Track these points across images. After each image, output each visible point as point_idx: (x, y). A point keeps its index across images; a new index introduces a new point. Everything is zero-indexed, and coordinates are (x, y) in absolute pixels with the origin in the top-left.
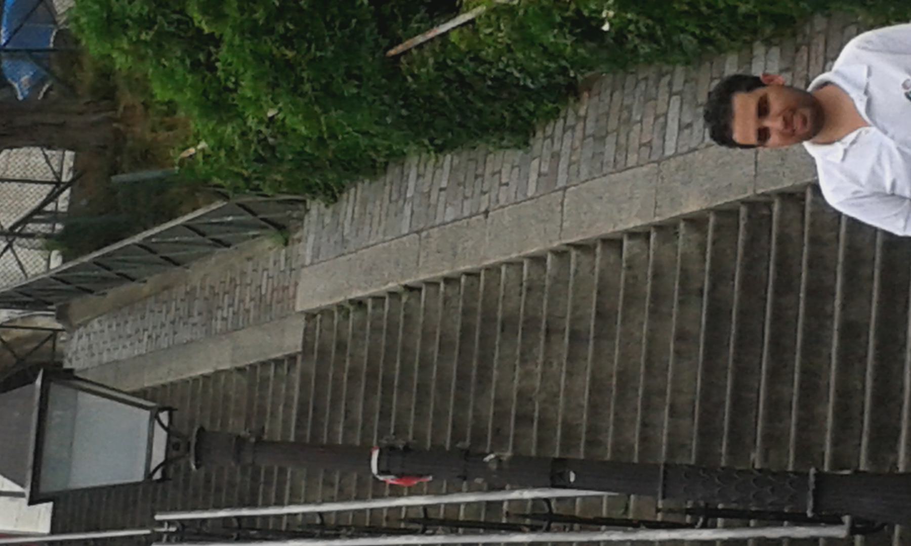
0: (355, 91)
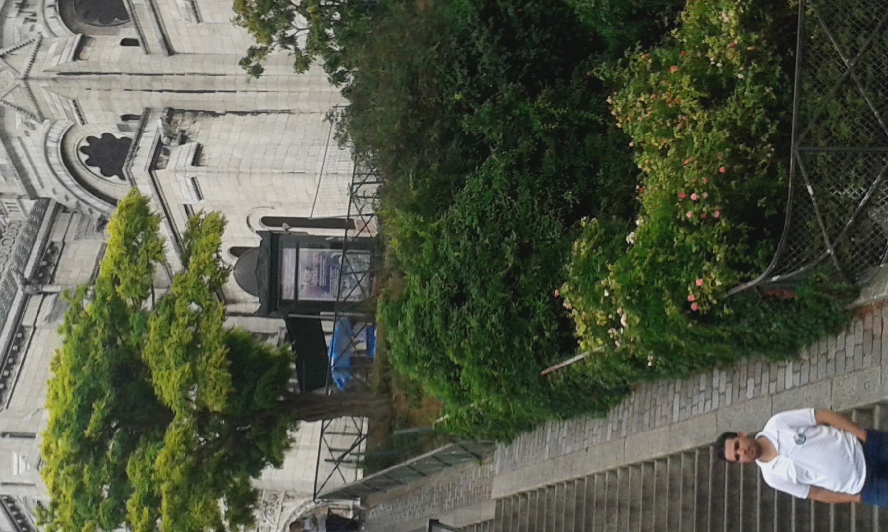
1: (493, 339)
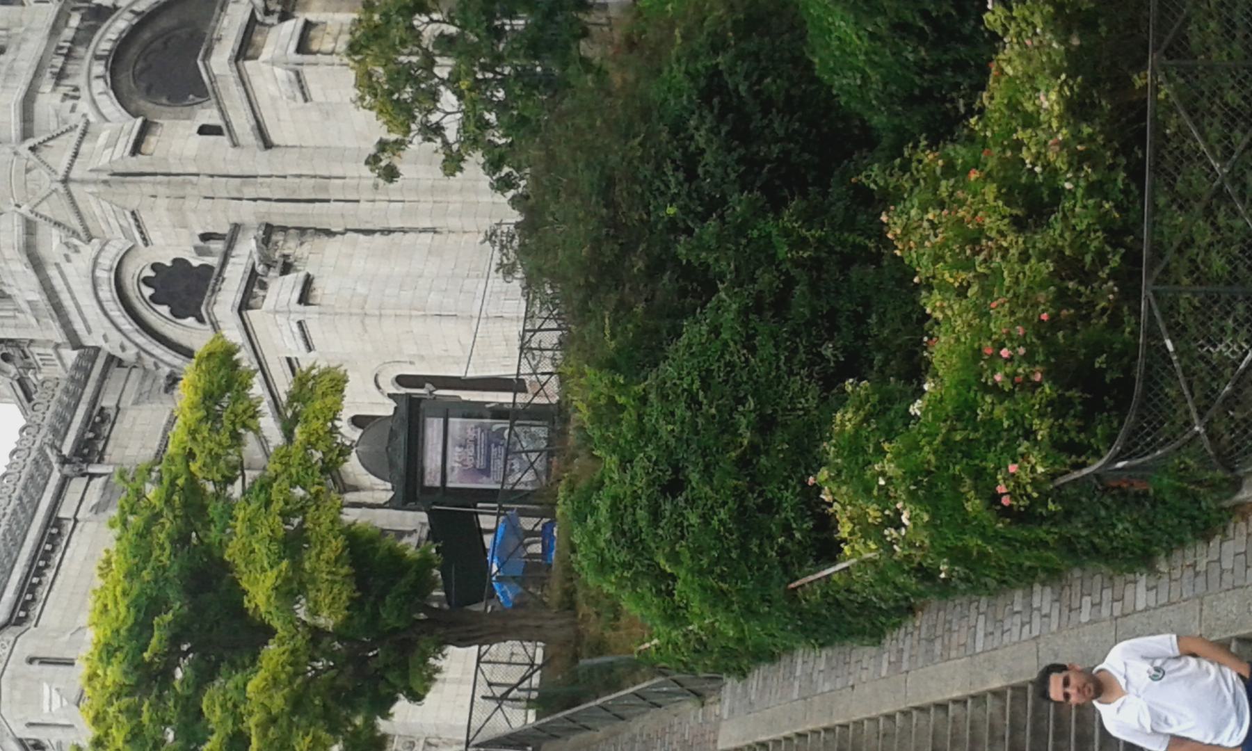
1: (721, 541)
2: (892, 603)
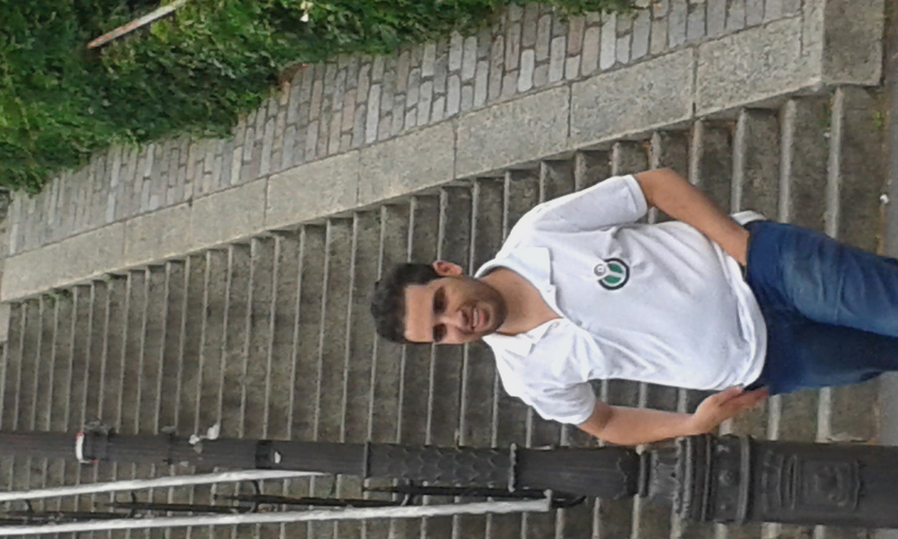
0: (55, 82)
2: (245, 71)
